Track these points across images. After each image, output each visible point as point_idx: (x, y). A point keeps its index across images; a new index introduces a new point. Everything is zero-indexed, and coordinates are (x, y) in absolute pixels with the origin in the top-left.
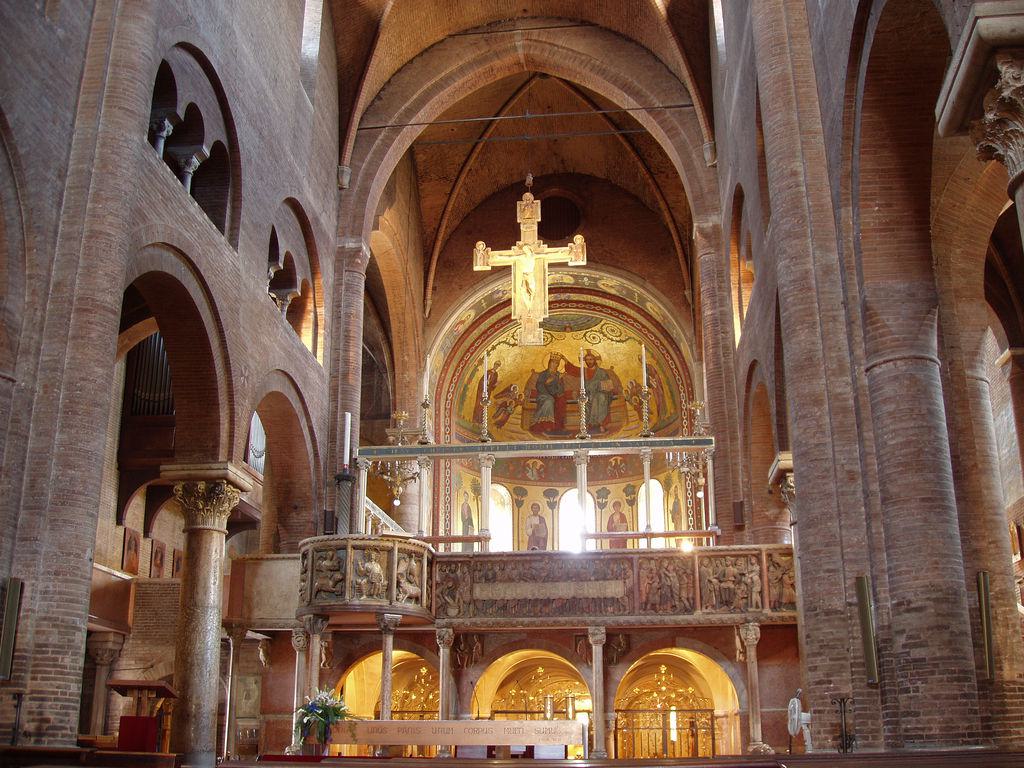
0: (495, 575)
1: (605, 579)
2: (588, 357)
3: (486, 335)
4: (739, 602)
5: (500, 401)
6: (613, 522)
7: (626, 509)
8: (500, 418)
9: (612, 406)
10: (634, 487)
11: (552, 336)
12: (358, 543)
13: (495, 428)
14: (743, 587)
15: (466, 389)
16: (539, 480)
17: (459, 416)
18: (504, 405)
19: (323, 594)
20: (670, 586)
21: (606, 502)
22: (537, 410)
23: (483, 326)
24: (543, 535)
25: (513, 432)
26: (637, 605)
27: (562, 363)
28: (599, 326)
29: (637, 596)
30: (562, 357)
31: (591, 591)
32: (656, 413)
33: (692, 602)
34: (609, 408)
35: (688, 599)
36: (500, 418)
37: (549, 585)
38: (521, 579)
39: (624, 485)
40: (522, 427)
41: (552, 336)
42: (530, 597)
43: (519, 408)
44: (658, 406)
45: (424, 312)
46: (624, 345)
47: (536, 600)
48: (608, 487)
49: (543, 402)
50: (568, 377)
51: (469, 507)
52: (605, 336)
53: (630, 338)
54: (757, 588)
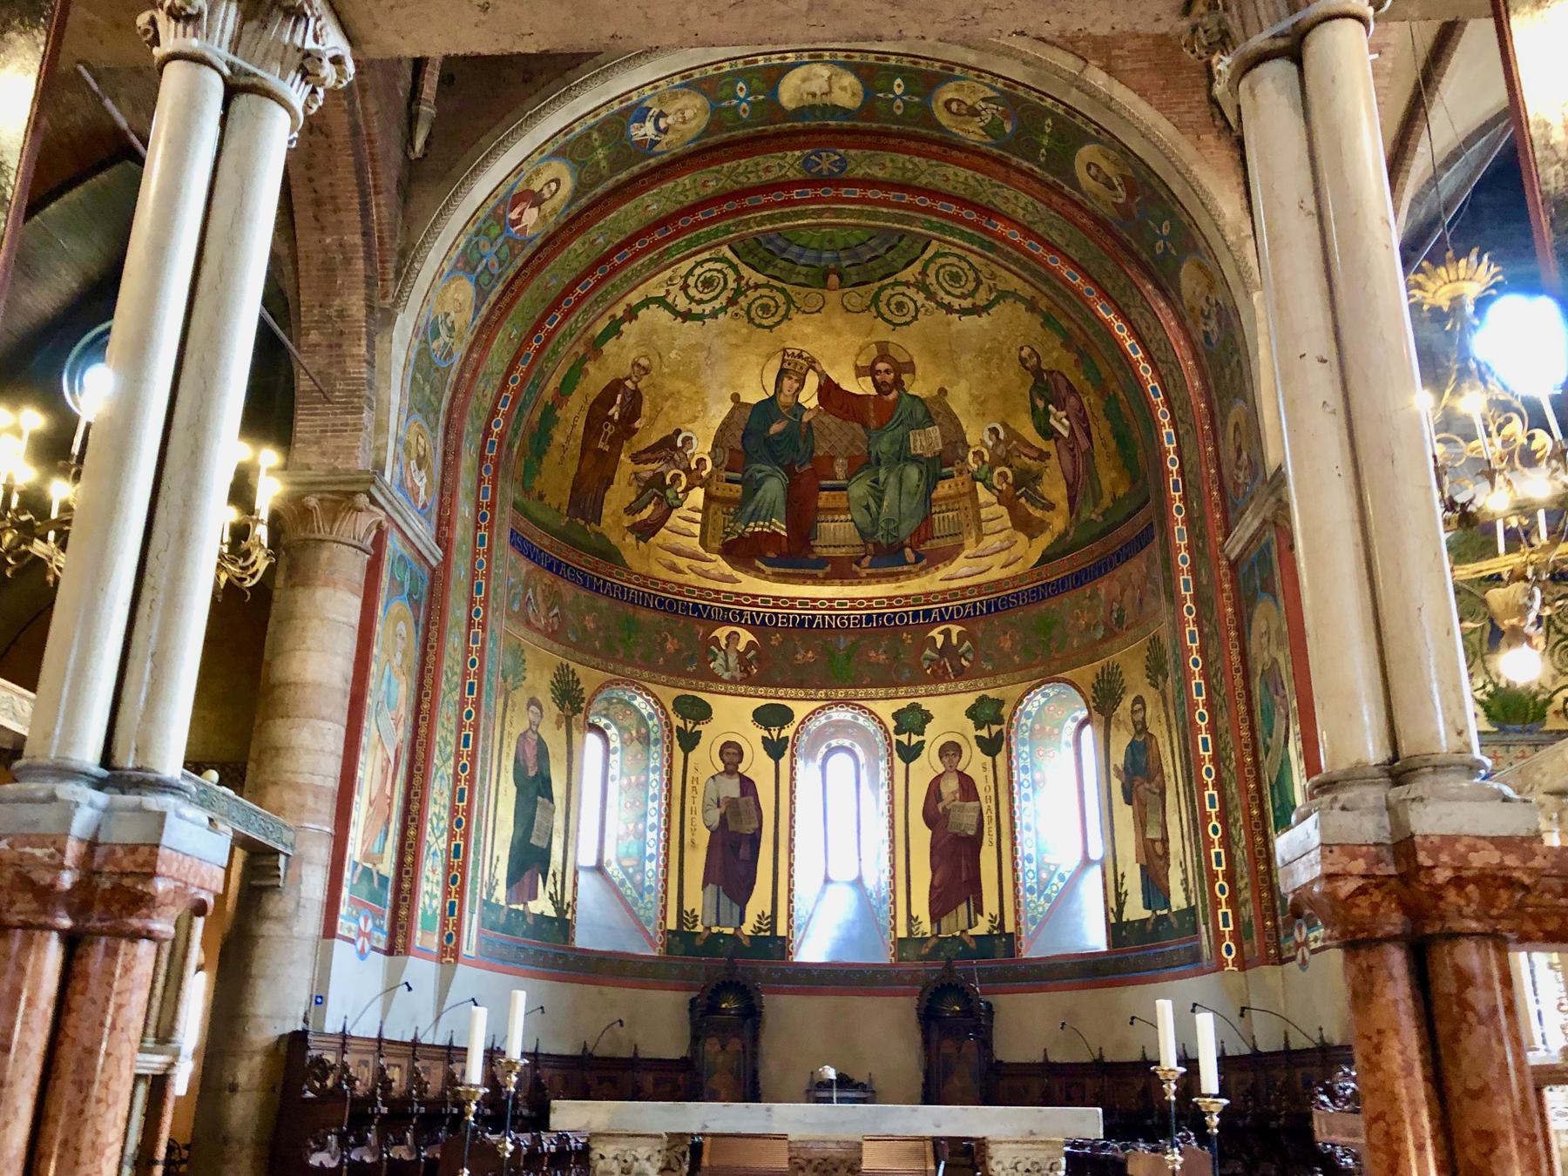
2: (881, 366)
3: (604, 265)
5: (648, 470)
6: (939, 798)
7: (975, 763)
8: (646, 513)
9: (934, 496)
10: (1000, 703)
11: (790, 301)
13: (631, 539)
15: (549, 417)
16: (742, 682)
17: (527, 491)
18: (657, 481)
21: (921, 744)
22: (741, 503)
23: (600, 236)
24: (748, 828)
25: (678, 552)
27: (812, 381)
28: (916, 267)
30: (812, 364)
32: (1064, 505)
34: (928, 501)
36: (646, 513)
39: (969, 699)
40: (703, 543)
41: (790, 301)
43: (697, 496)
44: (1069, 486)
45: (410, 141)
46: (984, 320)
48: (926, 704)
49: (761, 482)
50: (827, 419)
51: (541, 743)
52: (931, 296)
53: (1003, 295)
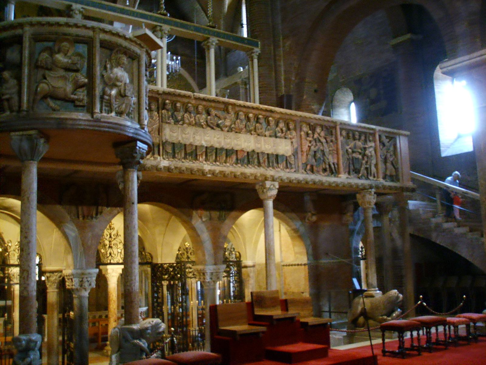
0: (183, 119)
1: (276, 137)
4: (363, 171)
12: (107, 37)
14: (366, 159)
19: (52, 103)
20: (323, 151)
26: (300, 164)
29: (300, 156)
31: (267, 146)
33: (336, 166)
35: (334, 164)
37: (232, 134)
38: (208, 125)
42: (217, 145)
47: (222, 149)
54: (374, 162)
